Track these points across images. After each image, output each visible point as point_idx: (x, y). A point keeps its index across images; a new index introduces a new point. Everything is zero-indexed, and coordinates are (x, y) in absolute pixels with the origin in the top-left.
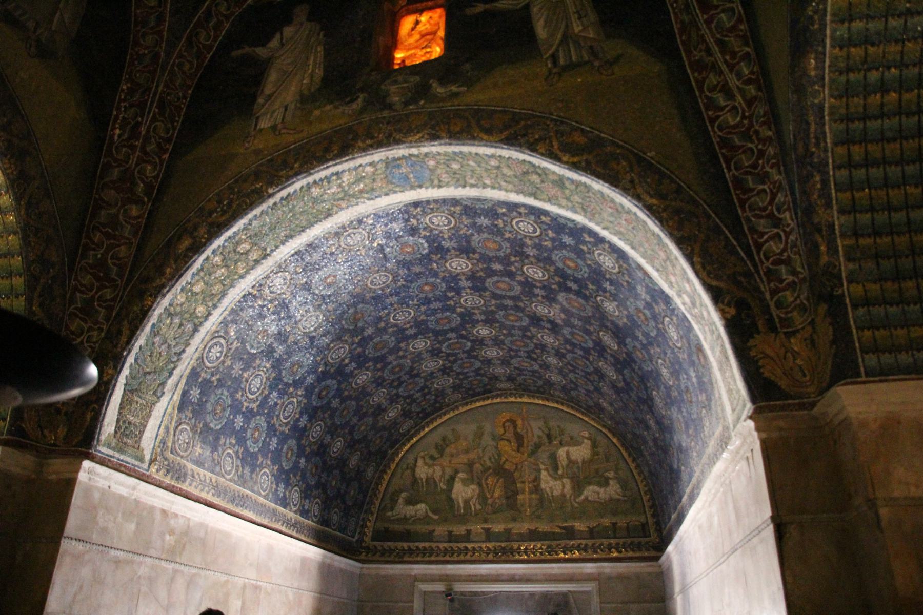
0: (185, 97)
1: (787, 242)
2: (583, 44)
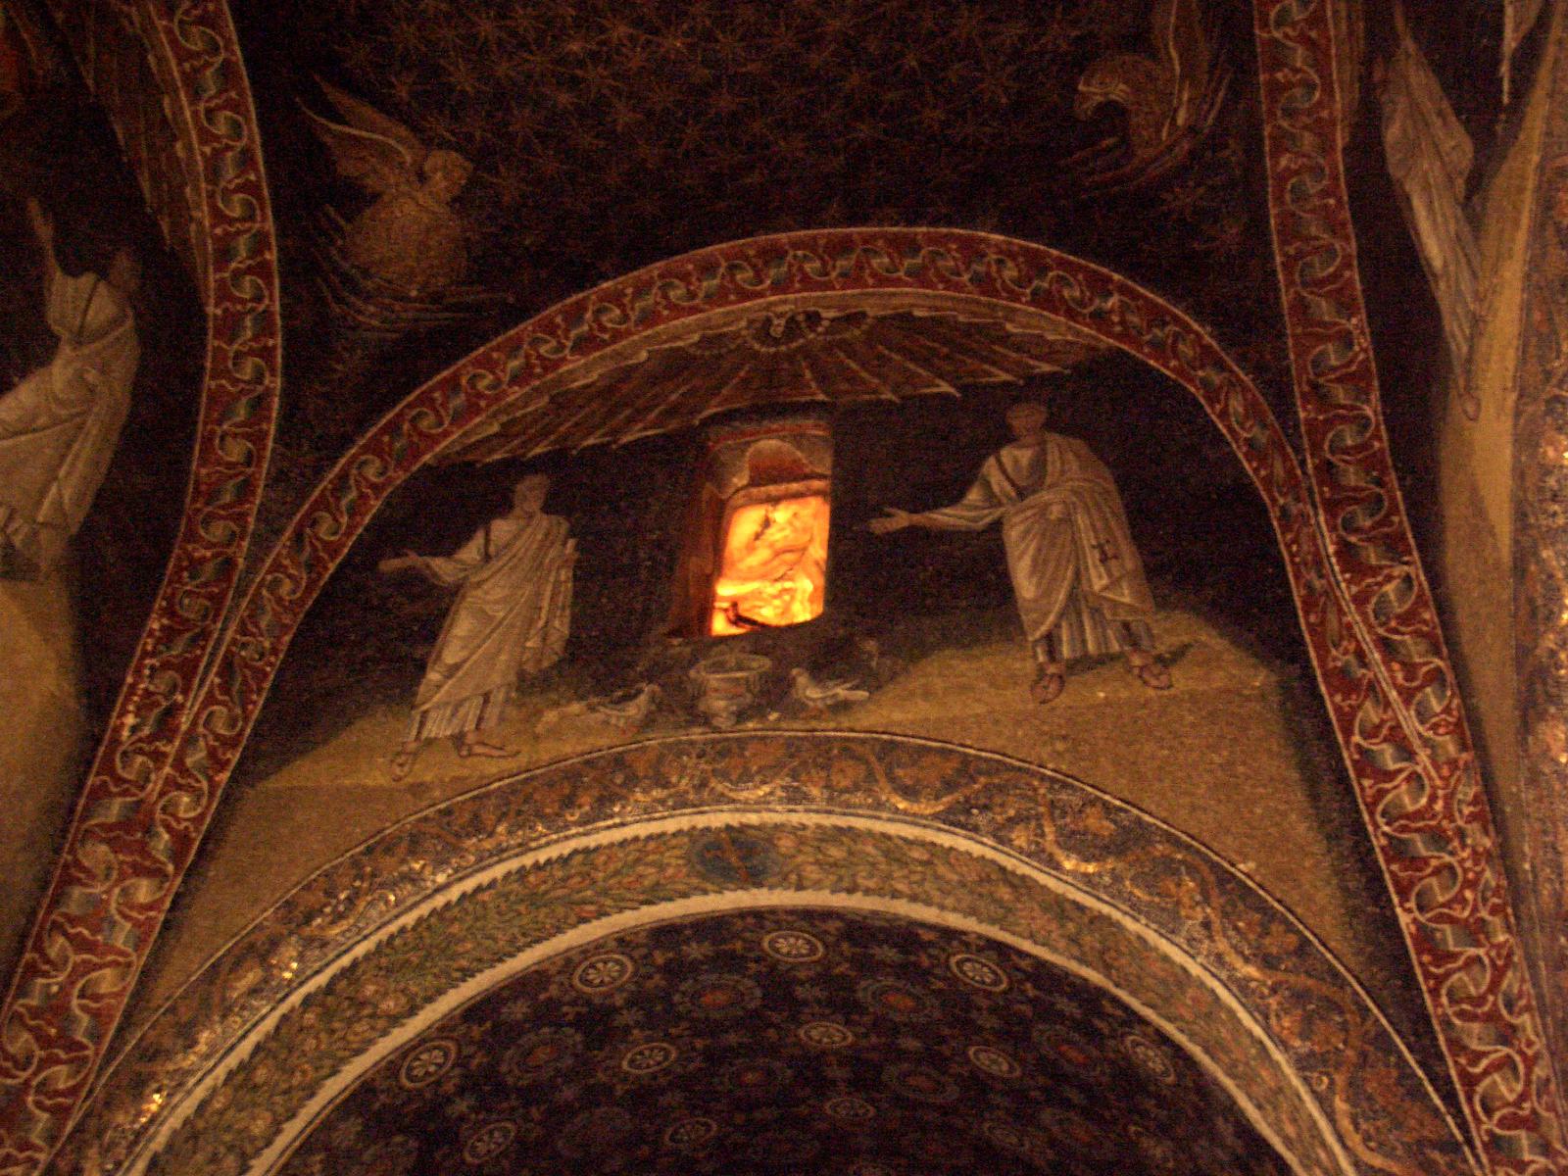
0: (275, 651)
1: (1528, 1083)
2: (1109, 617)
